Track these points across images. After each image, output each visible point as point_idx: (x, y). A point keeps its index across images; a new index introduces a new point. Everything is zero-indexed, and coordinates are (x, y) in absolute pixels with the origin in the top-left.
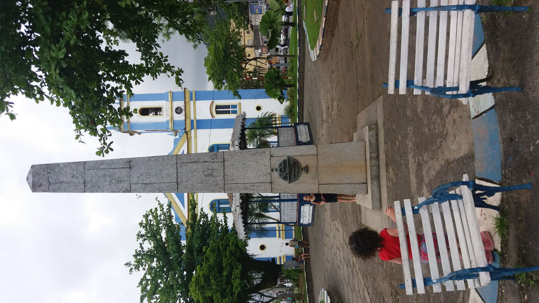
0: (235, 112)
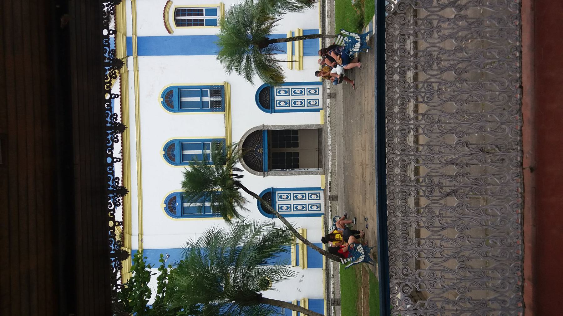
0: (212, 23)
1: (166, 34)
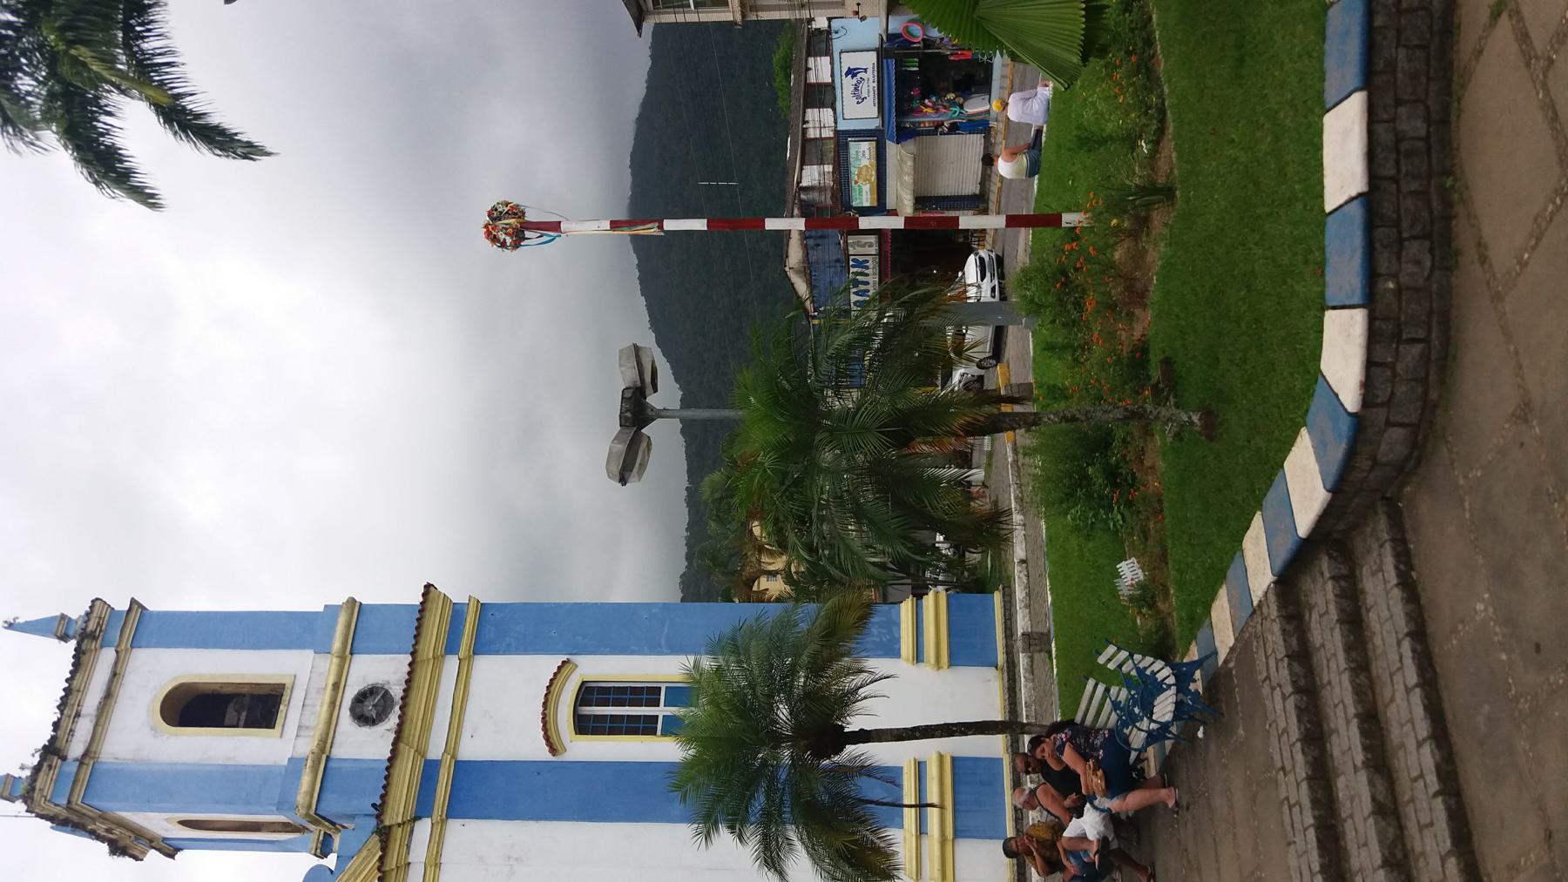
1: (543, 754)
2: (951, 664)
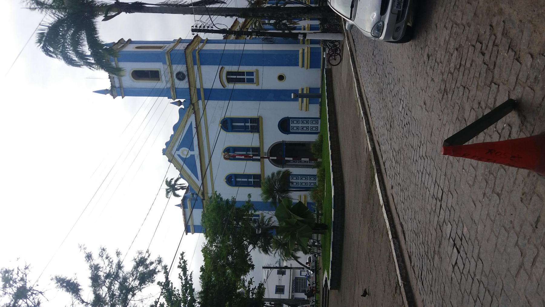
1: (222, 87)
2: (310, 68)
